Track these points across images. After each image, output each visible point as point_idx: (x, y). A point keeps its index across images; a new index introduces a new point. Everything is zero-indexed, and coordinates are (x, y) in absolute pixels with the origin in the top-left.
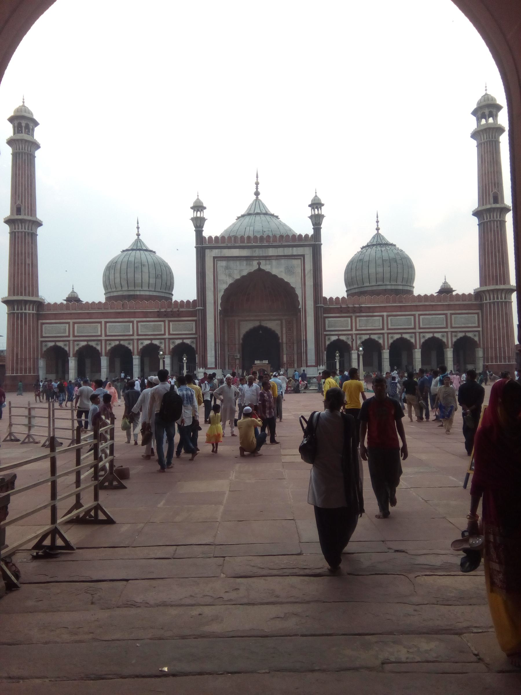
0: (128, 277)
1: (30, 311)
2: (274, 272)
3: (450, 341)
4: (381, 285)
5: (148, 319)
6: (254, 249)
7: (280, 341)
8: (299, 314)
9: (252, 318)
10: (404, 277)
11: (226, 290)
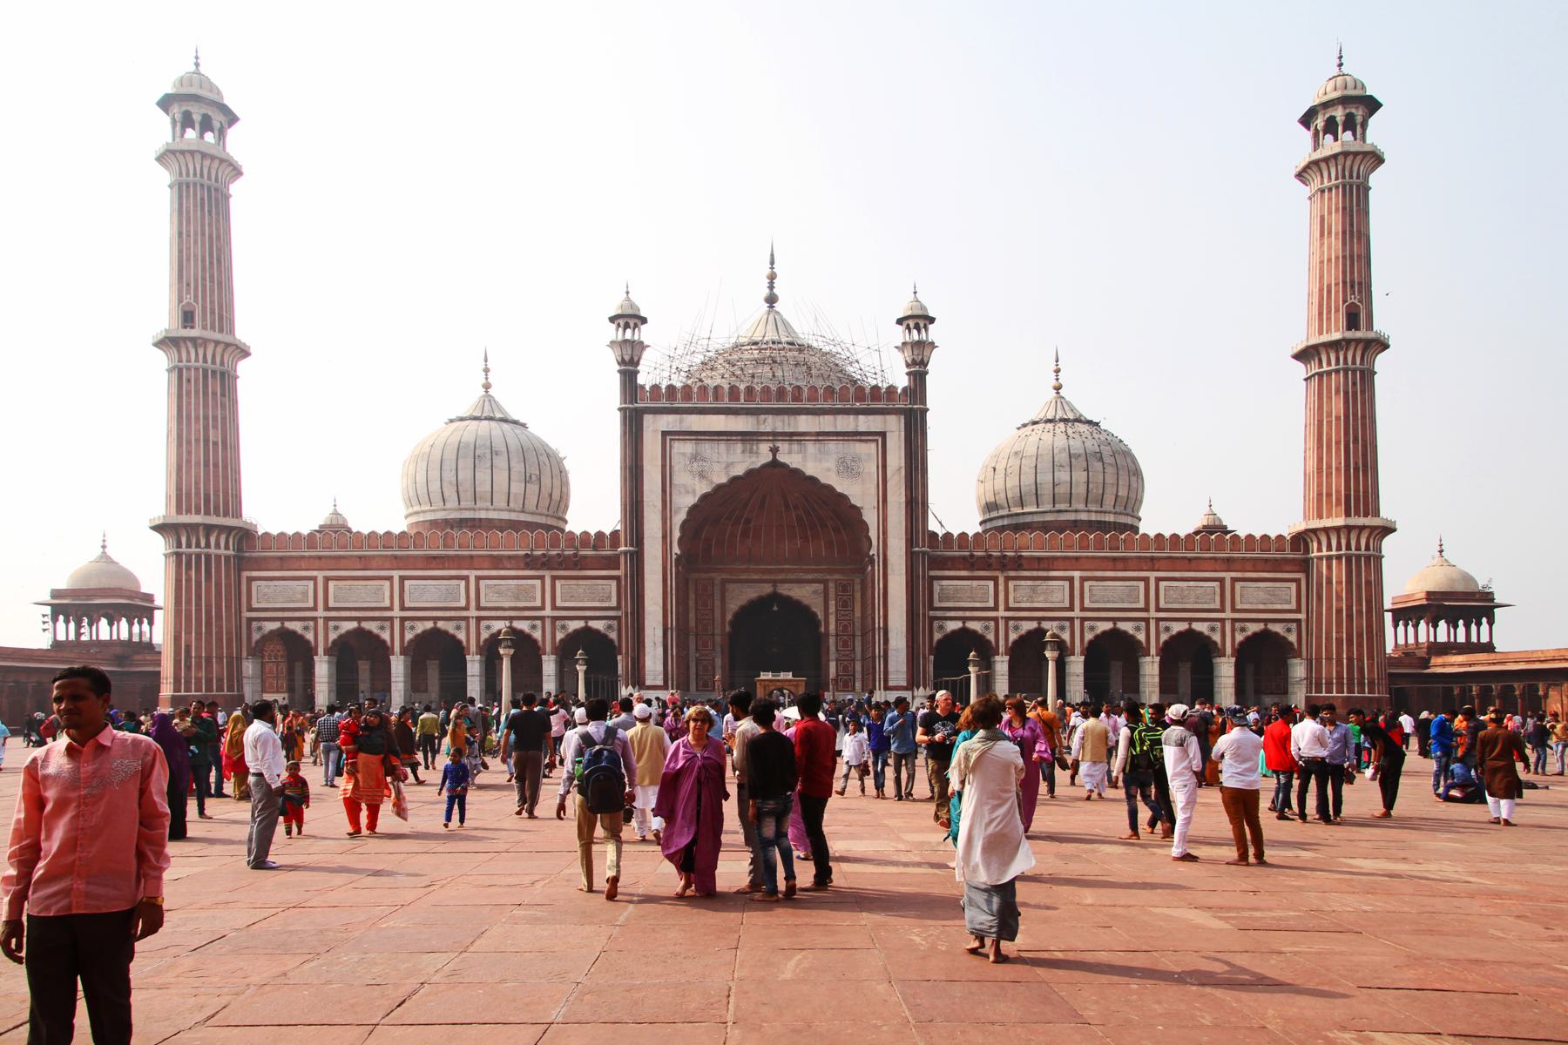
1: (223, 549)
3: (1229, 641)
5: (502, 573)
8: (870, 568)
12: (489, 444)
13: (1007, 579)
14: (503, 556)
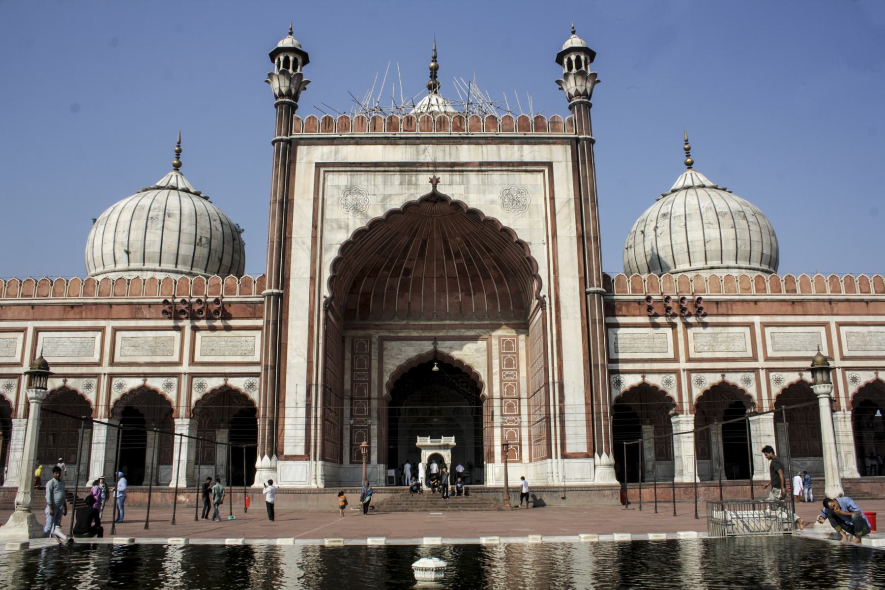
0: (131, 239)
2: (473, 201)
4: (719, 268)
6: (422, 147)
7: (486, 392)
9: (415, 334)
10: (765, 252)
11: (345, 248)
12: (163, 206)
13: (688, 325)
14: (143, 304)
